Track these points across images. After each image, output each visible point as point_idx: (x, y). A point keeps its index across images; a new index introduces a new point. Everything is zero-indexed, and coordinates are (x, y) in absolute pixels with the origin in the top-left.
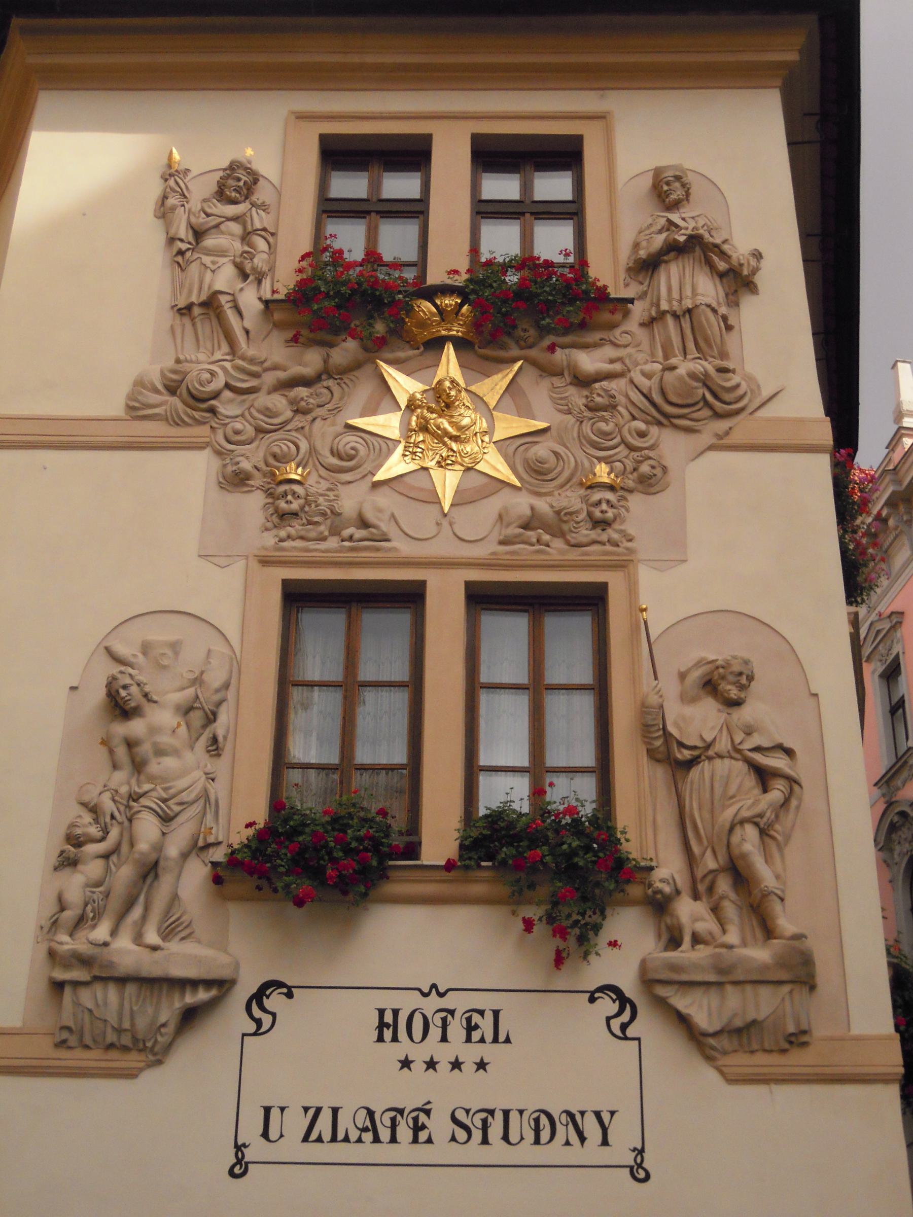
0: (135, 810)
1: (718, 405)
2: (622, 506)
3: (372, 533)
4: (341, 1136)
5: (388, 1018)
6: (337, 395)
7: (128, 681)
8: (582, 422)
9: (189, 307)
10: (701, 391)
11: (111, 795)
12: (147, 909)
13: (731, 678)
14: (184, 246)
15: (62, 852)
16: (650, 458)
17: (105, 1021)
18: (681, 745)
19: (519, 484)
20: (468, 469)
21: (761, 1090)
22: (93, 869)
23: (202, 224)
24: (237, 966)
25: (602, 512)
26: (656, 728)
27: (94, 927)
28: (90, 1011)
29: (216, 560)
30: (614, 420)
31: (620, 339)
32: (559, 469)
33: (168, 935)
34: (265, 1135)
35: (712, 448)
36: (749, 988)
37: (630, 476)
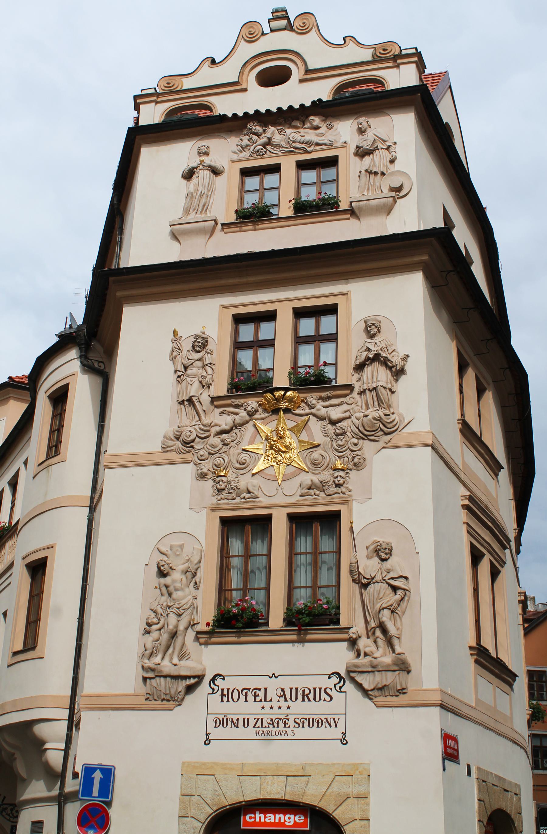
0: (168, 612)
2: (347, 476)
3: (252, 496)
6: (238, 436)
7: (164, 563)
8: (332, 441)
9: (183, 401)
11: (160, 607)
12: (174, 648)
13: (382, 550)
14: (180, 374)
15: (145, 629)
16: (359, 455)
17: (161, 691)
18: (364, 578)
19: (307, 470)
20: (288, 465)
21: (390, 709)
22: (155, 635)
23: (186, 364)
25: (338, 481)
26: (355, 571)
27: (156, 656)
28: (156, 687)
30: (345, 439)
31: (349, 401)
32: (323, 462)
33: (181, 658)
35: (383, 448)
36: (383, 672)
37: (351, 463)
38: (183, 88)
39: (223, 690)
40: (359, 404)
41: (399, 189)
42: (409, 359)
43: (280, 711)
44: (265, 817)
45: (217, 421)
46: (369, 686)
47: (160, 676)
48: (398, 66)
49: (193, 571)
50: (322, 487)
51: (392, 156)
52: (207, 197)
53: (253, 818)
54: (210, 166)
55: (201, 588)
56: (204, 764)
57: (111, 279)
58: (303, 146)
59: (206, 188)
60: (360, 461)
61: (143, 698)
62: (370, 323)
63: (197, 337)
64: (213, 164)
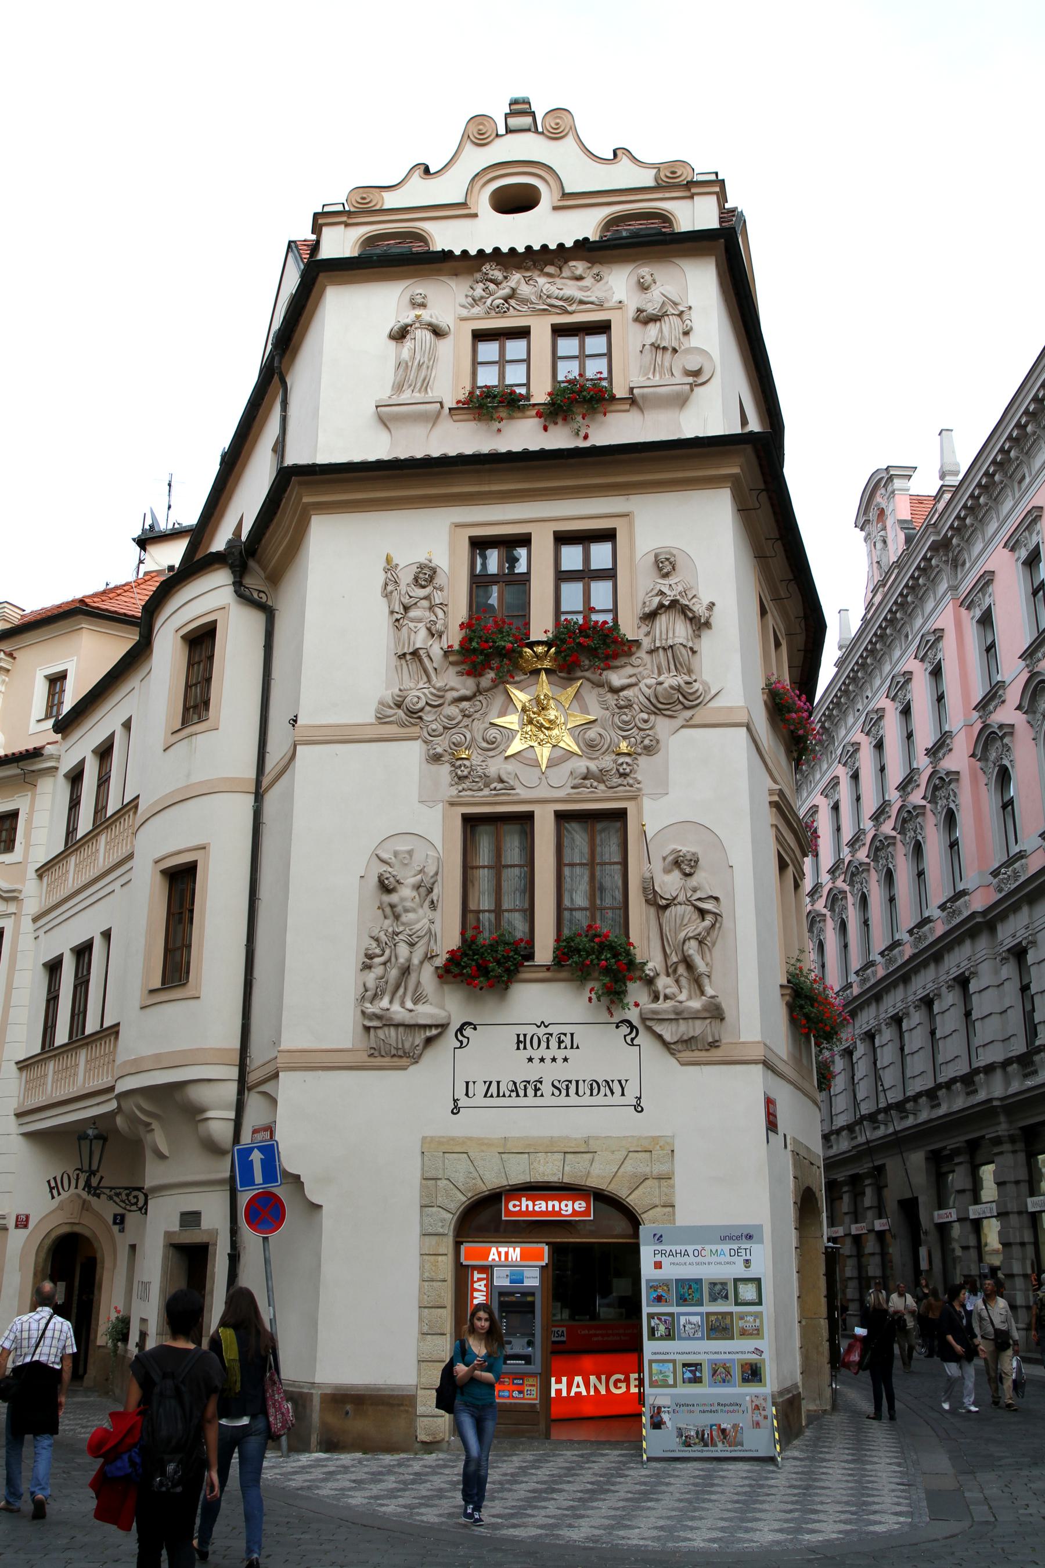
1: (686, 702)
4: (501, 1094)
5: (522, 1038)
6: (484, 705)
7: (388, 875)
9: (404, 655)
10: (678, 695)
12: (406, 989)
13: (686, 862)
14: (399, 616)
15: (364, 963)
18: (661, 897)
19: (580, 753)
20: (554, 746)
21: (697, 1068)
22: (379, 971)
24: (449, 1017)
27: (381, 999)
29: (427, 803)
34: (467, 1094)
35: (683, 727)
36: (690, 1021)
40: (649, 666)
41: (697, 373)
42: (715, 608)
44: (534, 1205)
47: (389, 1025)
48: (692, 197)
49: (428, 886)
50: (601, 777)
51: (687, 326)
52: (428, 367)
53: (518, 1206)
54: (430, 325)
55: (439, 909)
56: (453, 1139)
58: (561, 303)
59: (426, 355)
62: (662, 557)
63: (421, 567)
64: (434, 321)
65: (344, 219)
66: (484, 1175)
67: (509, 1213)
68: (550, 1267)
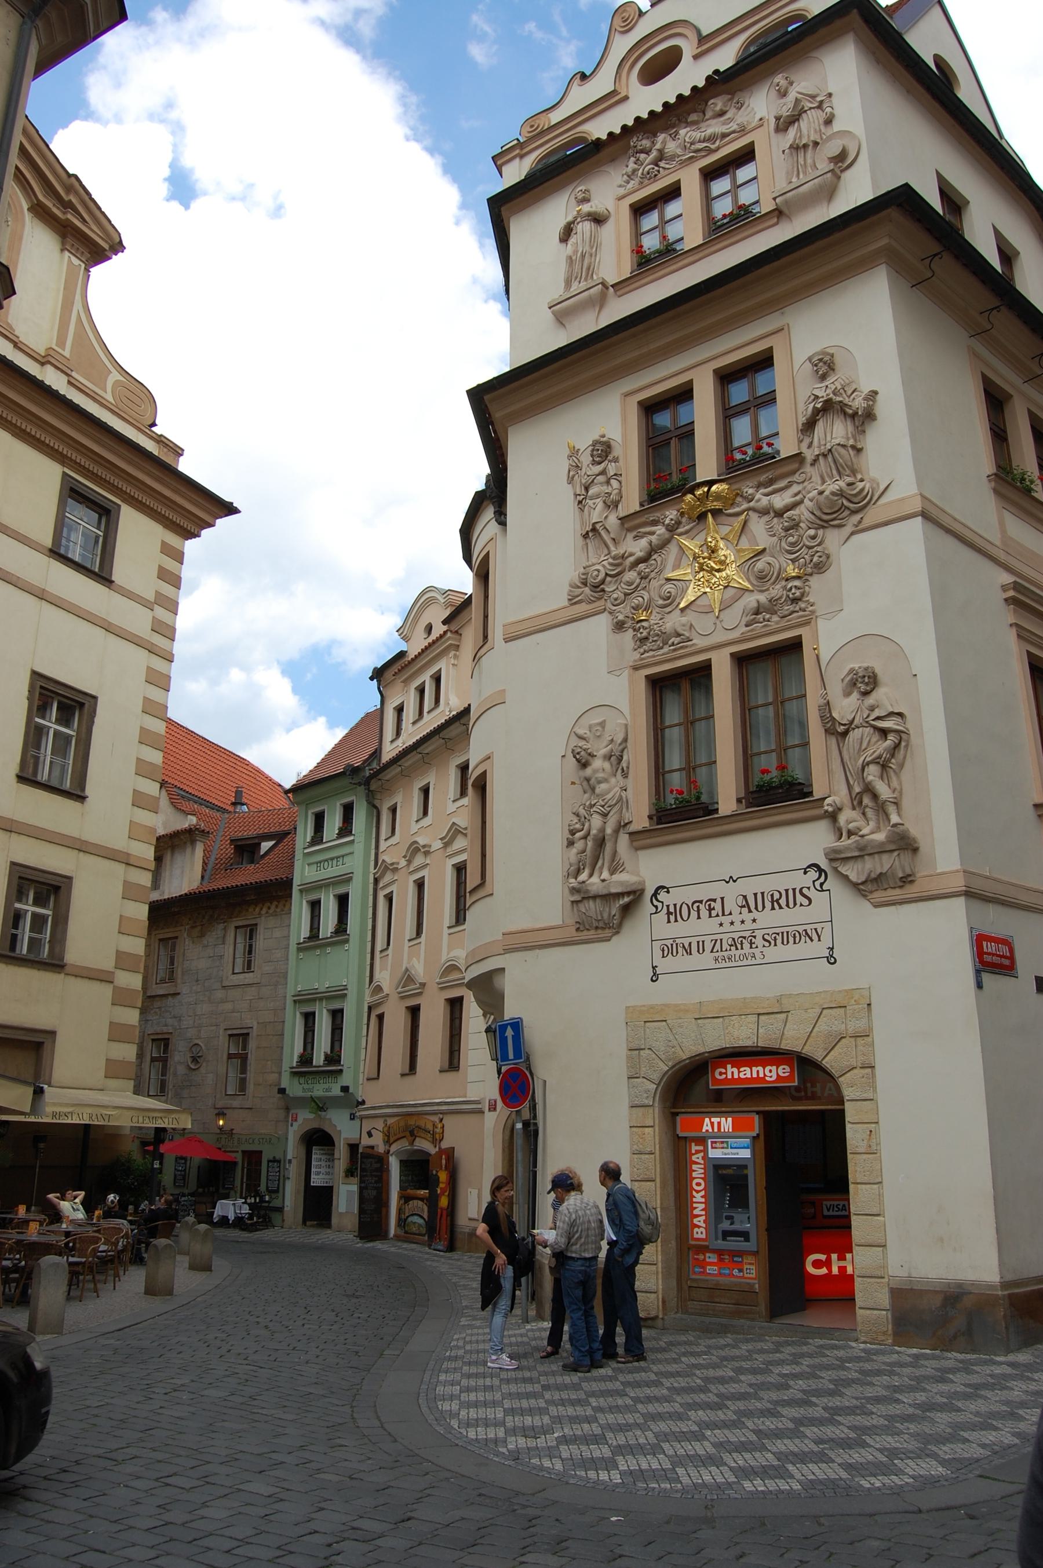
6: (659, 563)
7: (579, 750)
9: (587, 533)
13: (860, 680)
16: (818, 552)
20: (725, 587)
21: (892, 908)
22: (579, 845)
35: (852, 534)
36: (876, 856)
38: (552, 124)
39: (668, 906)
40: (813, 479)
42: (879, 397)
43: (743, 927)
44: (739, 1072)
45: (630, 550)
46: (858, 878)
49: (618, 754)
52: (591, 255)
54: (589, 214)
56: (652, 1007)
57: (487, 398)
58: (705, 144)
60: (821, 559)
61: (573, 929)
63: (595, 443)
64: (593, 209)
65: (517, 151)
66: (682, 1042)
67: (715, 1080)
68: (762, 1137)
